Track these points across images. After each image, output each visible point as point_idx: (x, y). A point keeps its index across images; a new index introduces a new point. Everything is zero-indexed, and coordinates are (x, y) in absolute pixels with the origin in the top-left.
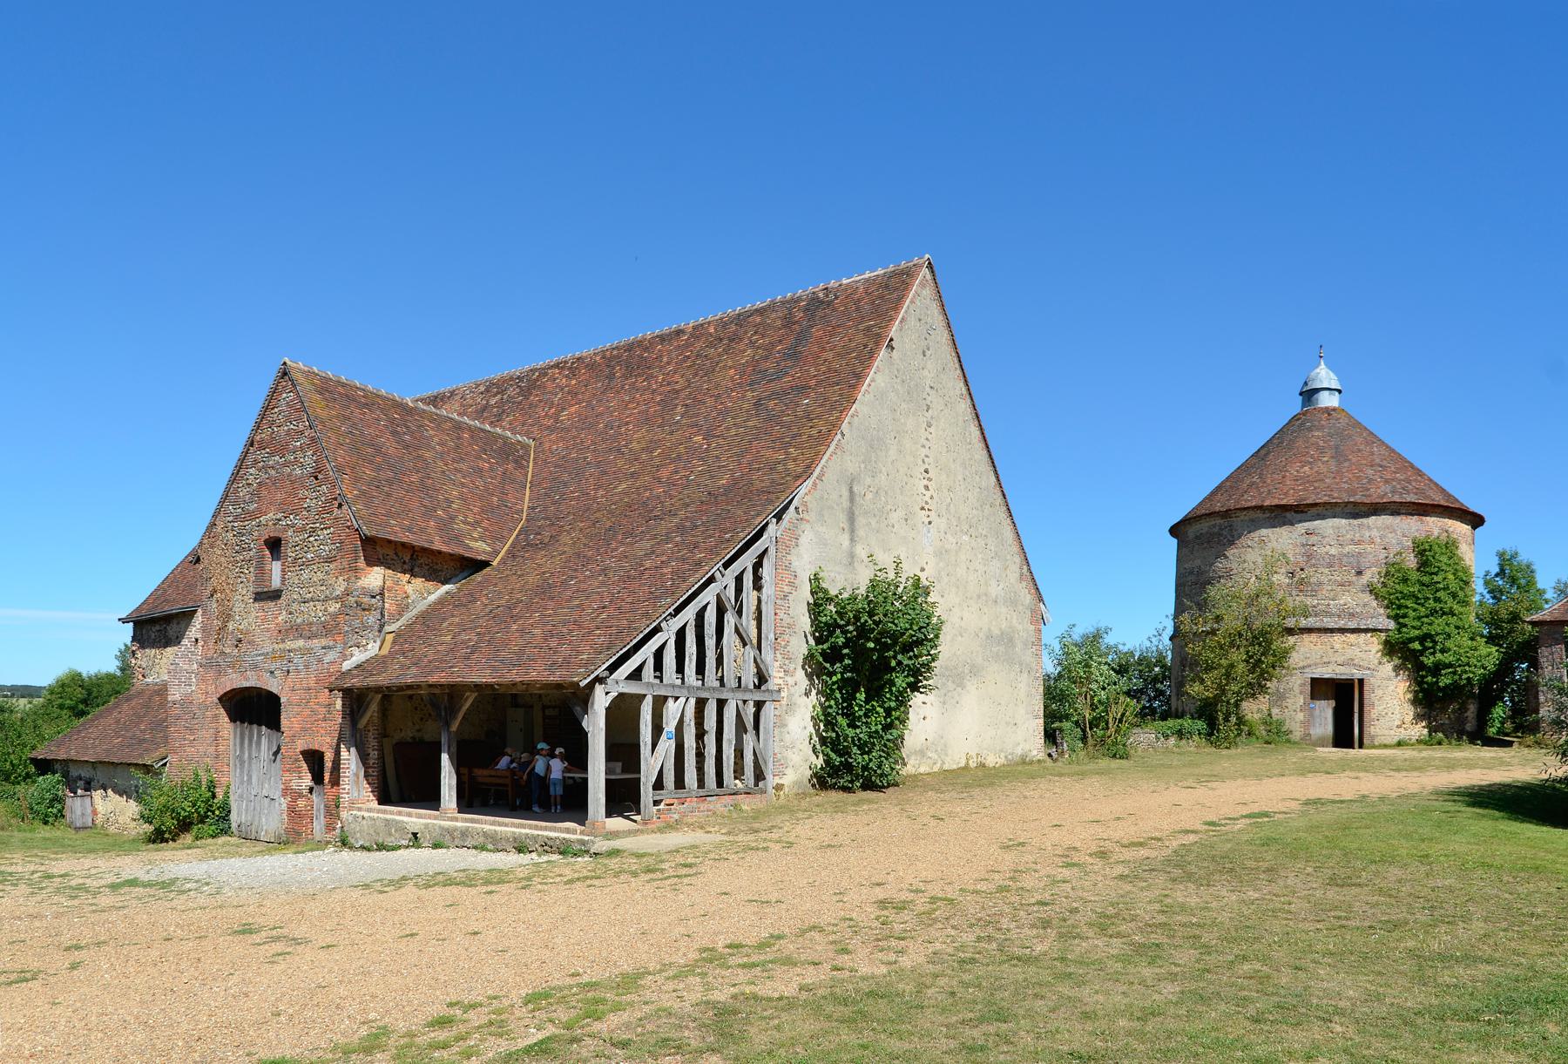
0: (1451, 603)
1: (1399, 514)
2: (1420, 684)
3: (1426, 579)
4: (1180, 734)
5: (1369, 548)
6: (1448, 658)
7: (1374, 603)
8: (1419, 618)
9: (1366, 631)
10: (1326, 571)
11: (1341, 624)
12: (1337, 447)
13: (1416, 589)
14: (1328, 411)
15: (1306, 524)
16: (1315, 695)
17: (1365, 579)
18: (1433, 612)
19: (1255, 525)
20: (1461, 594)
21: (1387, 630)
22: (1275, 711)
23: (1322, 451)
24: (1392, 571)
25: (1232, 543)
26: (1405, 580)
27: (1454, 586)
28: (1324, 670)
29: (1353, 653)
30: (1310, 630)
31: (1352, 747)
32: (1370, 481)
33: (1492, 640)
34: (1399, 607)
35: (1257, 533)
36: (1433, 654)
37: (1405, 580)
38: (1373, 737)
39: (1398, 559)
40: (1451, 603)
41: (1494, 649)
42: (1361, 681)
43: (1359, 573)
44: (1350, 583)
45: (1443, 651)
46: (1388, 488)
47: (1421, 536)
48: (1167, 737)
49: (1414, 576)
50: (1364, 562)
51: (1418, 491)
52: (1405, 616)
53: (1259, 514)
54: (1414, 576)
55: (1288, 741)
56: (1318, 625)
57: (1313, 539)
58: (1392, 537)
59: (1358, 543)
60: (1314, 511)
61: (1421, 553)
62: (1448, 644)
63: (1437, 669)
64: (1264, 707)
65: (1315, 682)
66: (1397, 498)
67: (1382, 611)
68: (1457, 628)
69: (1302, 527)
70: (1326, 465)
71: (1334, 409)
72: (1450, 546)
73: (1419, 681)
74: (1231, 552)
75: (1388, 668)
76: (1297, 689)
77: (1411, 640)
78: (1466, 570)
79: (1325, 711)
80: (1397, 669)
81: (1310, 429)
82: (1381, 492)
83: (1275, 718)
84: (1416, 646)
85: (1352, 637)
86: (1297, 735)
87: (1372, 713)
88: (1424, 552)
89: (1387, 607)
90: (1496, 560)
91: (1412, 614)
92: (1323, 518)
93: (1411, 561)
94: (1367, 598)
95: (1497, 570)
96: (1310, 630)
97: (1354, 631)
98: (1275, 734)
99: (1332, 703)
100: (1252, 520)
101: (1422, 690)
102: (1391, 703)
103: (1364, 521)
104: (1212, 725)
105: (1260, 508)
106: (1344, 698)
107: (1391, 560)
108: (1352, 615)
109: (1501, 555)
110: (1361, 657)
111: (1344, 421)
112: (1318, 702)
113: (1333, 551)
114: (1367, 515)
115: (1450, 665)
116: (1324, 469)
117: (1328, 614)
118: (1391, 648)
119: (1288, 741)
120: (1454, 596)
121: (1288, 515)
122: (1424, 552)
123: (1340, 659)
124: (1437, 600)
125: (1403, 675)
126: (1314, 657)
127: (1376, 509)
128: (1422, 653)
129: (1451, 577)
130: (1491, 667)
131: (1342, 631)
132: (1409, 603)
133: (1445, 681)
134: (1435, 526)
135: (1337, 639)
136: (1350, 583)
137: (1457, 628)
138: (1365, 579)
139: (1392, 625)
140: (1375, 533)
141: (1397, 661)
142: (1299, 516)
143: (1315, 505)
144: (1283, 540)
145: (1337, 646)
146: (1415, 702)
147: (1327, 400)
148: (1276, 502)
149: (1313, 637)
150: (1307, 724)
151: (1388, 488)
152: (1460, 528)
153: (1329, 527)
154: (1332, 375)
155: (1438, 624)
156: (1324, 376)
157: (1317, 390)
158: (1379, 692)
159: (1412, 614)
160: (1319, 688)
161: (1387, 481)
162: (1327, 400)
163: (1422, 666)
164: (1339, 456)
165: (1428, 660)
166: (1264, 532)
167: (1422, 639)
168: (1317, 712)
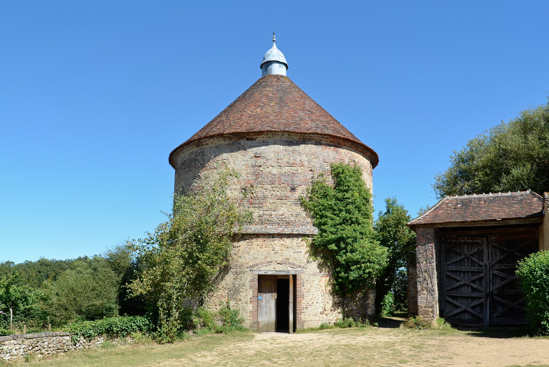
0: (357, 215)
1: (321, 144)
2: (336, 278)
3: (340, 195)
4: (110, 332)
5: (300, 170)
6: (356, 256)
7: (304, 214)
8: (335, 225)
9: (298, 236)
10: (269, 187)
11: (280, 230)
12: (281, 98)
13: (333, 202)
14: (278, 77)
15: (255, 149)
16: (260, 290)
17: (297, 194)
18: (345, 221)
19: (219, 150)
20: (363, 208)
21: (313, 235)
22: (232, 303)
23: (270, 99)
24: (317, 190)
25: (203, 166)
26: (325, 196)
27: (359, 201)
28: (267, 268)
29: (287, 253)
30: (257, 236)
31: (289, 333)
32: (301, 119)
33: (384, 243)
34: (322, 217)
35: (219, 158)
36: (345, 253)
37: (325, 196)
38: (303, 323)
39: (321, 179)
40: (357, 215)
41: (386, 249)
42: (295, 277)
43: (293, 189)
44: (287, 197)
45: (352, 251)
46: (314, 125)
47: (337, 163)
48: (89, 337)
49: (332, 192)
50: (297, 182)
51: (334, 129)
52: (325, 224)
53: (221, 142)
54: (332, 192)
55: (241, 329)
56: (263, 231)
57: (260, 161)
58: (316, 161)
59: (292, 165)
60: (260, 138)
61: (337, 175)
62: (356, 245)
63: (347, 267)
64: (224, 300)
65: (262, 278)
66: (319, 131)
67: (309, 220)
68: (361, 233)
69: (252, 152)
70: (272, 108)
71: (282, 76)
72: (357, 172)
73: (335, 276)
74: (203, 174)
75: (314, 266)
76: (248, 284)
77: (330, 242)
78: (367, 191)
79: (269, 301)
80: (320, 266)
81: (264, 87)
82: (308, 126)
83: (232, 309)
84: (333, 247)
85: (288, 241)
86: (247, 324)
87: (302, 303)
88: (338, 174)
89: (313, 217)
90: (385, 204)
91: (330, 222)
92: (266, 144)
93: (330, 182)
94: (299, 209)
95: (386, 211)
96: (257, 236)
97: (290, 236)
98: (231, 323)
99: (275, 295)
100: (217, 147)
101: (338, 284)
102: (315, 293)
103: (296, 148)
104: (155, 319)
105: (221, 135)
106: (281, 288)
107: (316, 180)
108: (288, 223)
109: (387, 201)
110: (294, 256)
111: (288, 84)
112: (264, 295)
113: (275, 171)
114: (298, 144)
115: (357, 262)
116: (270, 110)
117: (272, 223)
118: (318, 249)
119: (241, 329)
120: (359, 208)
121: (242, 142)
122: (338, 174)
123: (279, 260)
124: (348, 212)
125: (325, 271)
126: (256, 257)
127: (304, 138)
128: (337, 252)
129: (357, 194)
130: (385, 264)
131: (281, 236)
132: (329, 214)
133: (353, 275)
134: (347, 157)
135: (277, 243)
136: (287, 197)
137: (361, 233)
138: (297, 194)
139: (316, 231)
140: (304, 158)
141: (320, 260)
142: (249, 143)
143: (260, 133)
144: (238, 161)
145: (277, 248)
146: (334, 293)
147: (278, 70)
148: (233, 131)
149: (260, 241)
150: (256, 312)
151: (314, 125)
152: (363, 162)
153: (272, 151)
154: (281, 54)
155: (348, 231)
156: (275, 53)
157: (270, 63)
158: (307, 286)
159: (330, 222)
160: (265, 283)
161: (313, 121)
162: (278, 70)
163: (337, 264)
164: (281, 102)
165: (342, 259)
166: (225, 155)
167: (337, 241)
168: (264, 303)
